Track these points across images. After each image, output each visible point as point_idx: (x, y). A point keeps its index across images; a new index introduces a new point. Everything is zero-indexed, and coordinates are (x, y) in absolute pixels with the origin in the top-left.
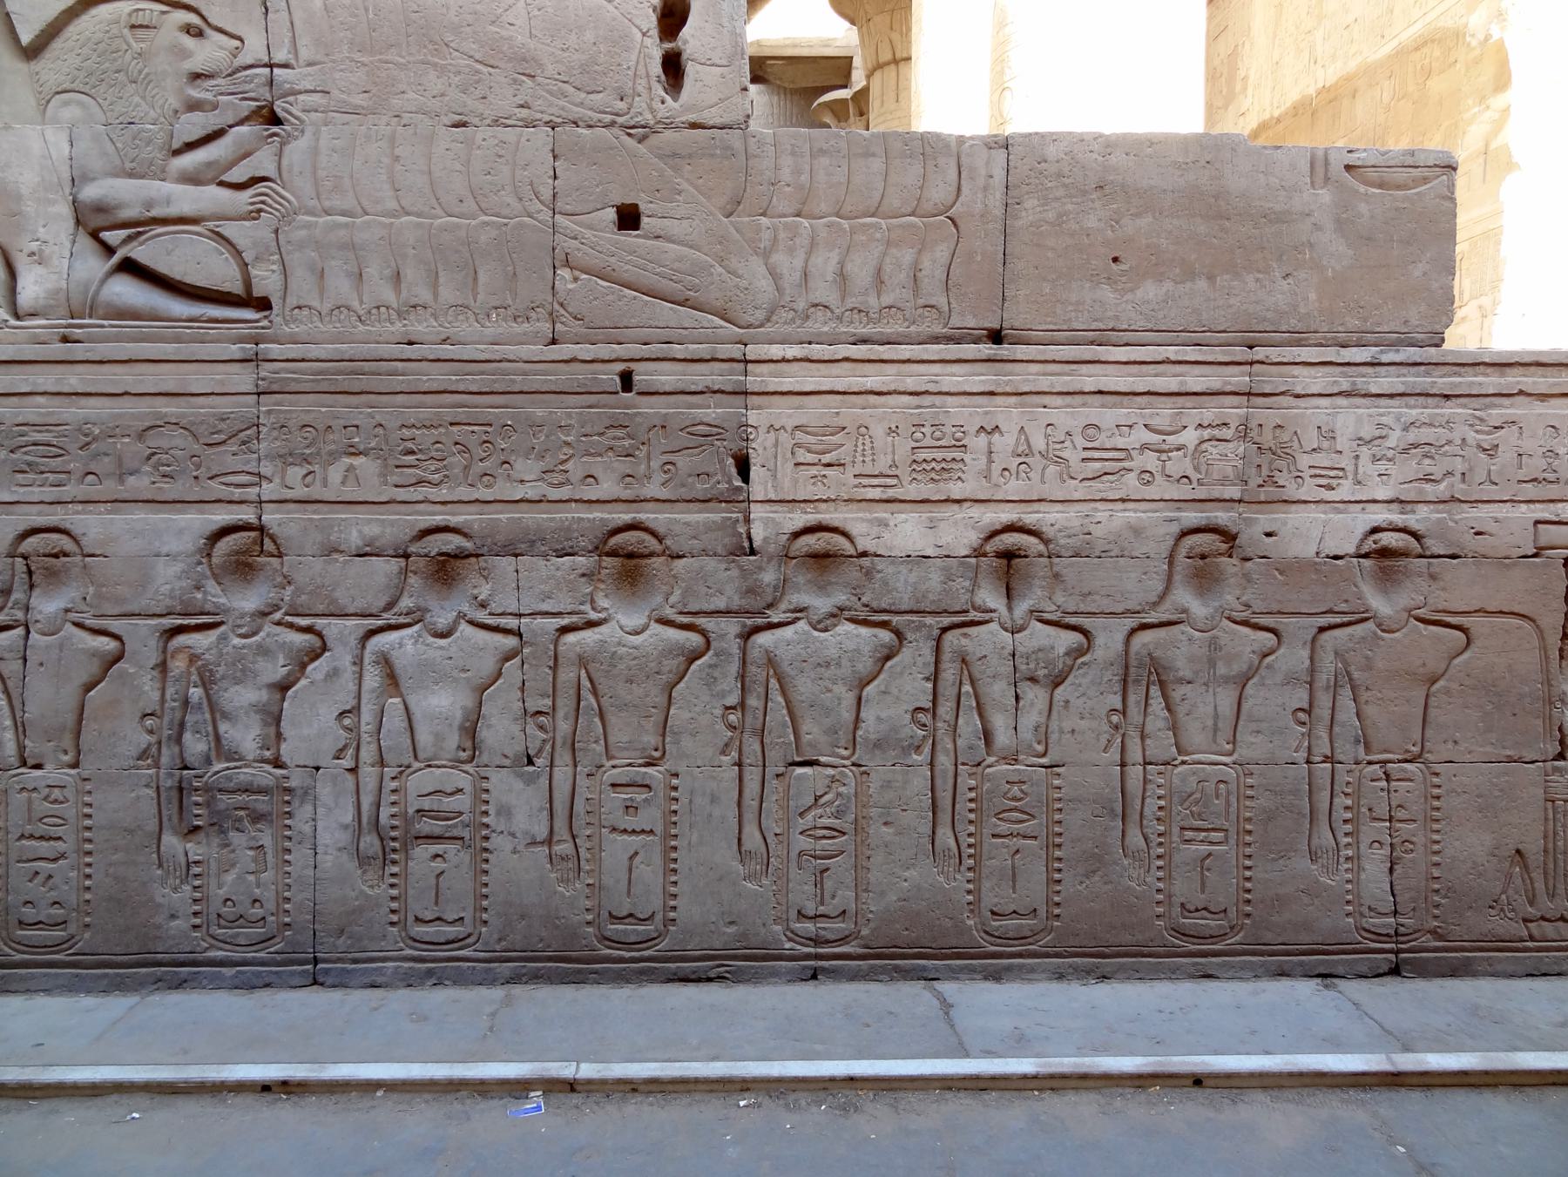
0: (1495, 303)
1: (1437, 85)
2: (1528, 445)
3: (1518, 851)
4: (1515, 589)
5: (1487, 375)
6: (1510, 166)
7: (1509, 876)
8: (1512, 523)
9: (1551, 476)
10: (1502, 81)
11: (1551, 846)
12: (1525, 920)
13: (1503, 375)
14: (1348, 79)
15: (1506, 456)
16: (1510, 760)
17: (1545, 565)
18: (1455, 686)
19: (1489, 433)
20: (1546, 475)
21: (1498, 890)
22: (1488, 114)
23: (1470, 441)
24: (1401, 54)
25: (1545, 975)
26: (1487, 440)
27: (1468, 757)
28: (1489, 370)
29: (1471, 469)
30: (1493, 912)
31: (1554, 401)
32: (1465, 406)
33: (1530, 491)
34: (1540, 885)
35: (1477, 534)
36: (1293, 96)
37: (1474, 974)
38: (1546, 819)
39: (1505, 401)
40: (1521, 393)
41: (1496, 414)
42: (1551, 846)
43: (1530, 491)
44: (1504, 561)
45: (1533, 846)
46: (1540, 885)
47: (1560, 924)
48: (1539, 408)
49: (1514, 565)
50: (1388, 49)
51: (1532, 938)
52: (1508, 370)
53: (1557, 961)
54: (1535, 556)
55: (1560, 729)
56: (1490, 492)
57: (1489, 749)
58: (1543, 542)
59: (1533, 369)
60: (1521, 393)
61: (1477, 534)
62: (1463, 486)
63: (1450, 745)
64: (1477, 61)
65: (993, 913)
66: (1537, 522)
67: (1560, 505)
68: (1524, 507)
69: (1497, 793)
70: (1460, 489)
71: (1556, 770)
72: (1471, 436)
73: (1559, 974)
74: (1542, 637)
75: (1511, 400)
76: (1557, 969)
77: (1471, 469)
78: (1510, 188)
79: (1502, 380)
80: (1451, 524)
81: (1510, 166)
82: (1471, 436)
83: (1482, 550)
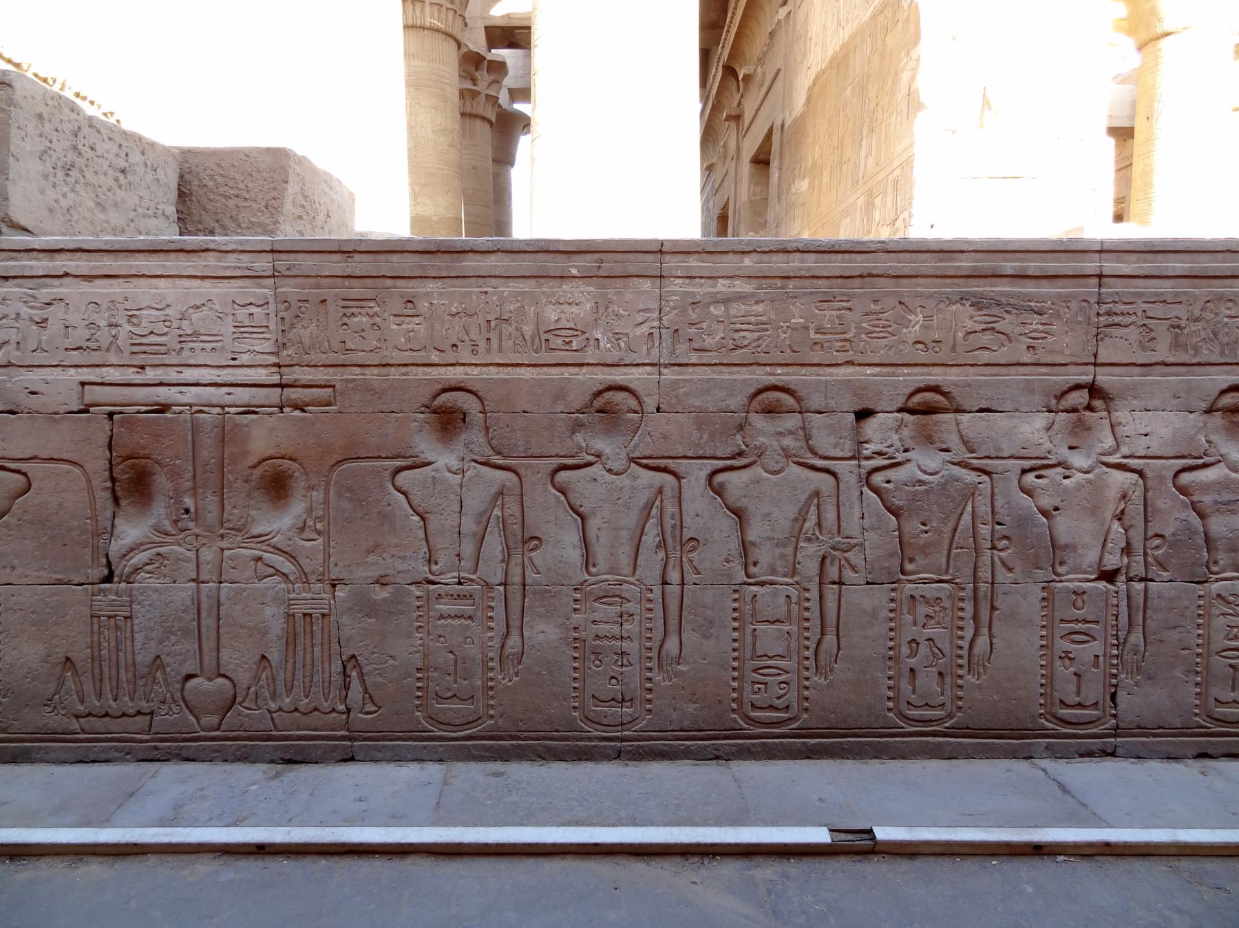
0: (910, 217)
1: (890, 40)
2: (72, 318)
3: (68, 659)
4: (59, 439)
5: (37, 259)
6: (920, 106)
7: (61, 681)
8: (60, 386)
9: (92, 345)
10: (916, 40)
11: (96, 654)
12: (77, 717)
13: (52, 260)
14: (853, 37)
15: (54, 327)
16: (60, 582)
17: (89, 419)
18: (13, 521)
19: (41, 309)
20: (89, 344)
21: (52, 691)
22: (911, 63)
23: (23, 315)
24: (875, 16)
25: (94, 761)
26: (38, 314)
27: (24, 581)
28: (41, 255)
29: (24, 339)
30: (50, 709)
31: (98, 282)
32: (21, 286)
33: (76, 357)
34: (89, 688)
35: (33, 393)
36: (830, 53)
37: (32, 761)
38: (92, 632)
39: (56, 282)
40: (66, 275)
41: (45, 293)
42: (96, 654)
43: (76, 357)
44: (52, 416)
45: (81, 654)
46: (89, 688)
47: (107, 719)
48: (85, 287)
49: (63, 419)
50: (869, 13)
51: (84, 731)
52: (57, 255)
53: (104, 750)
54: (86, 411)
55: (107, 556)
56: (39, 358)
57: (42, 573)
58: (88, 399)
59: (78, 254)
60: (66, 275)
61: (33, 393)
62: (18, 353)
63: (8, 571)
64: (907, 21)
65: (753, 705)
66: (83, 384)
67: (104, 369)
68: (72, 371)
69: (48, 610)
70: (15, 356)
71: (104, 591)
72: (25, 311)
73: (107, 761)
74: (89, 481)
75: (61, 280)
76: (103, 756)
77: (24, 339)
78: (922, 125)
79: (51, 264)
80: (9, 385)
81: (920, 106)
82: (25, 311)
83: (34, 407)
